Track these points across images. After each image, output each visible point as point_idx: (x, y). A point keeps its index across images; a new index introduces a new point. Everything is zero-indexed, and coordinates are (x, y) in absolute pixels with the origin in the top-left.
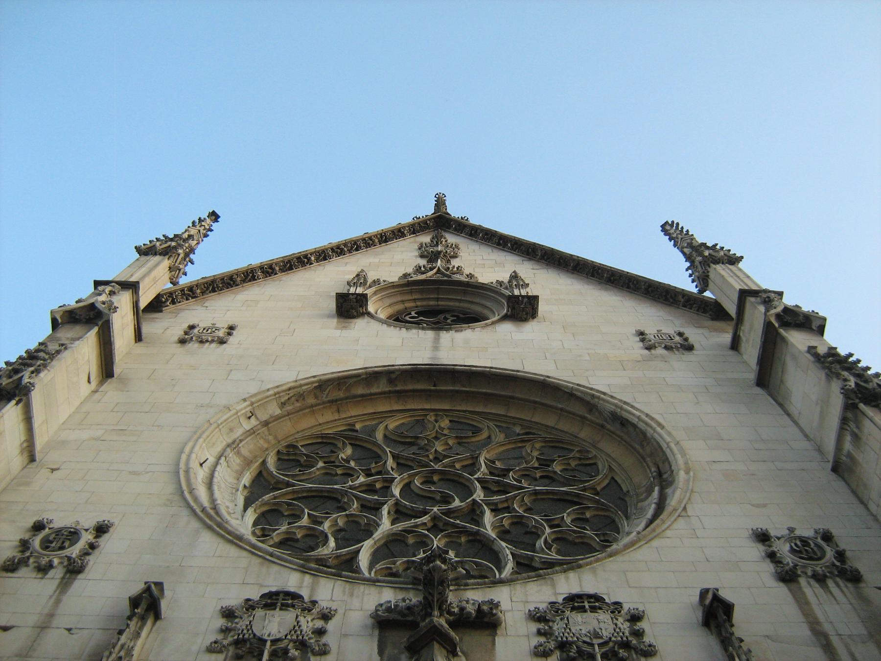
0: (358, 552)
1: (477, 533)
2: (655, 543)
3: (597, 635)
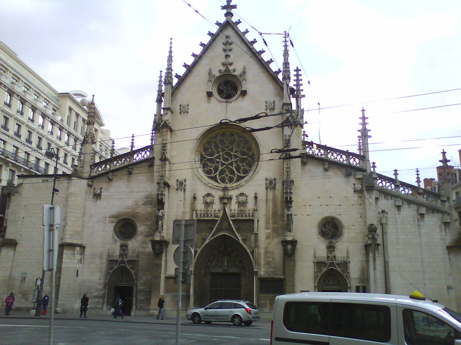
0: (217, 174)
1: (232, 169)
2: (253, 180)
3: (242, 201)
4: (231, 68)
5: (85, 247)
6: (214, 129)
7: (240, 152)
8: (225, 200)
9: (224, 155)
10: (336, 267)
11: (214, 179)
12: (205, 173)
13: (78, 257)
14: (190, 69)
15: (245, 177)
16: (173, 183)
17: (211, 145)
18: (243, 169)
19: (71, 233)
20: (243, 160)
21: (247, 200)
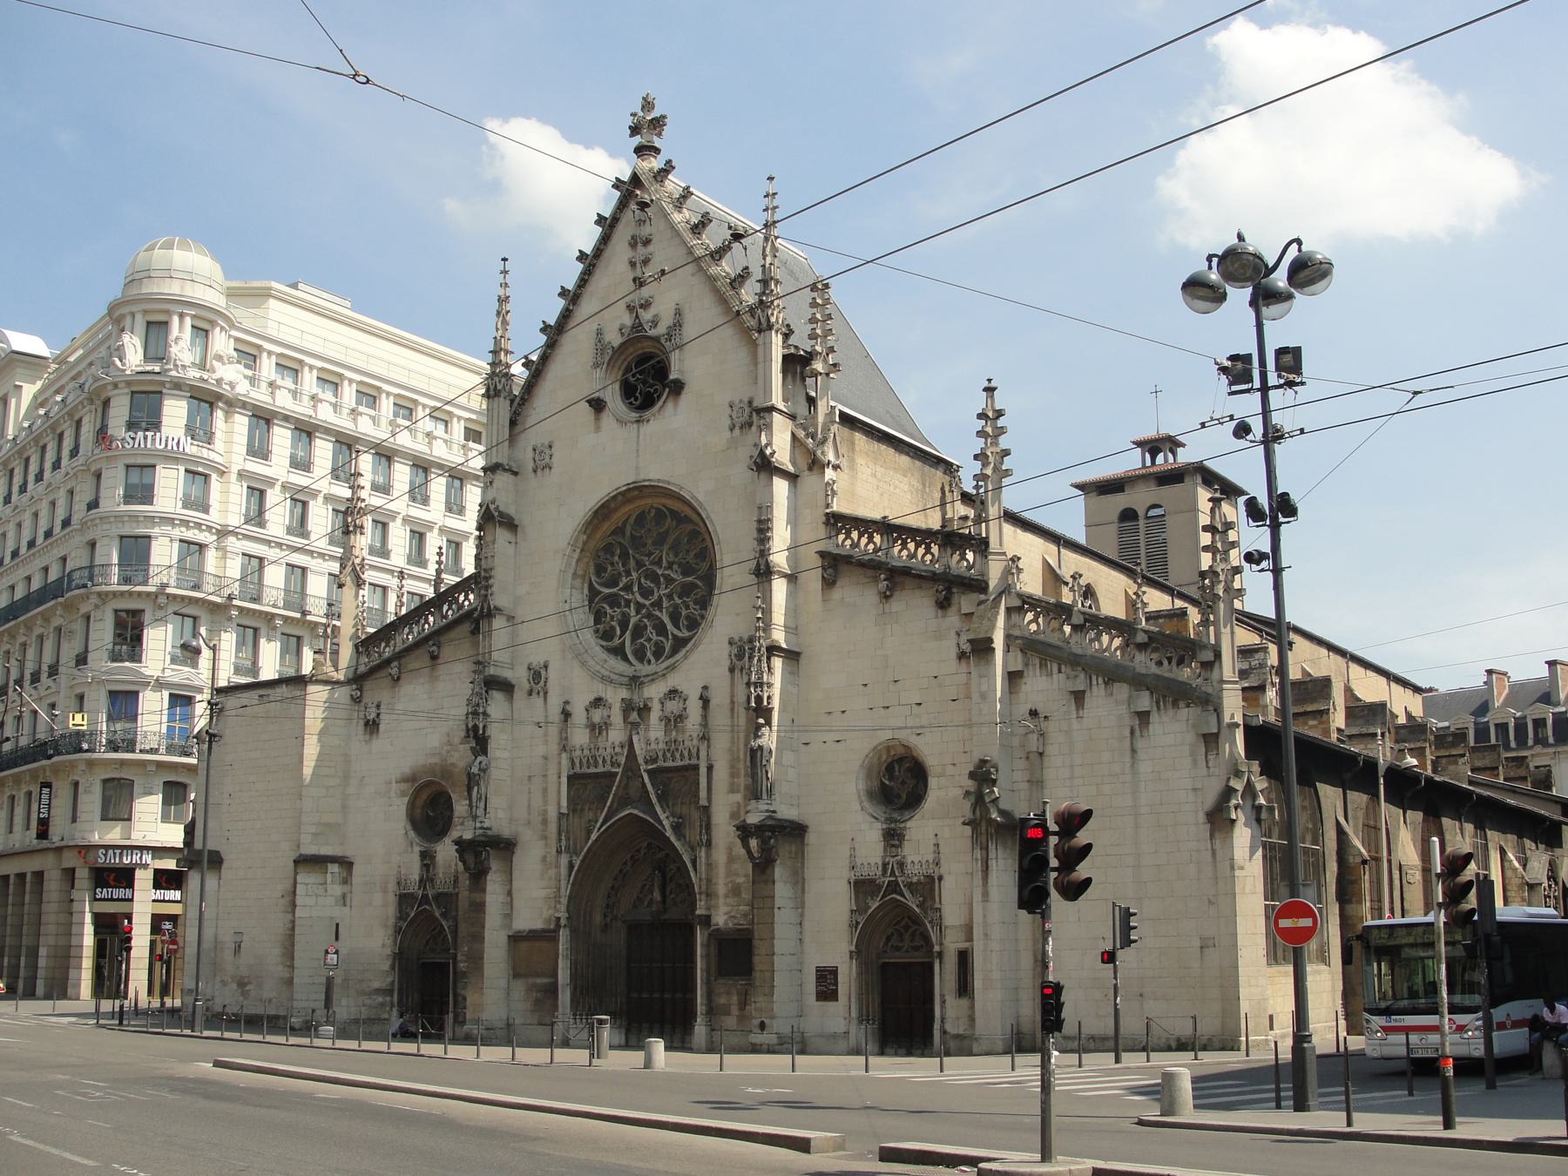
2: (699, 649)
4: (646, 316)
5: (352, 863)
6: (613, 505)
7: (680, 564)
8: (636, 712)
9: (642, 580)
10: (903, 896)
11: (619, 652)
12: (601, 638)
13: (338, 890)
14: (555, 333)
15: (690, 638)
16: (519, 676)
17: (613, 555)
18: (688, 617)
19: (313, 829)
20: (686, 590)
21: (685, 709)
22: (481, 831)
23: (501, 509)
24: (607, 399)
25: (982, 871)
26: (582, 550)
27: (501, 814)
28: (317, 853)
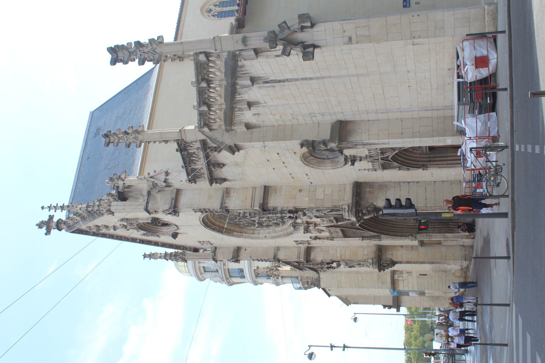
6: (217, 228)
16: (303, 247)
22: (374, 265)
23: (231, 258)
24: (172, 232)
25: (370, 145)
26: (241, 233)
27: (366, 252)
28: (390, 283)
